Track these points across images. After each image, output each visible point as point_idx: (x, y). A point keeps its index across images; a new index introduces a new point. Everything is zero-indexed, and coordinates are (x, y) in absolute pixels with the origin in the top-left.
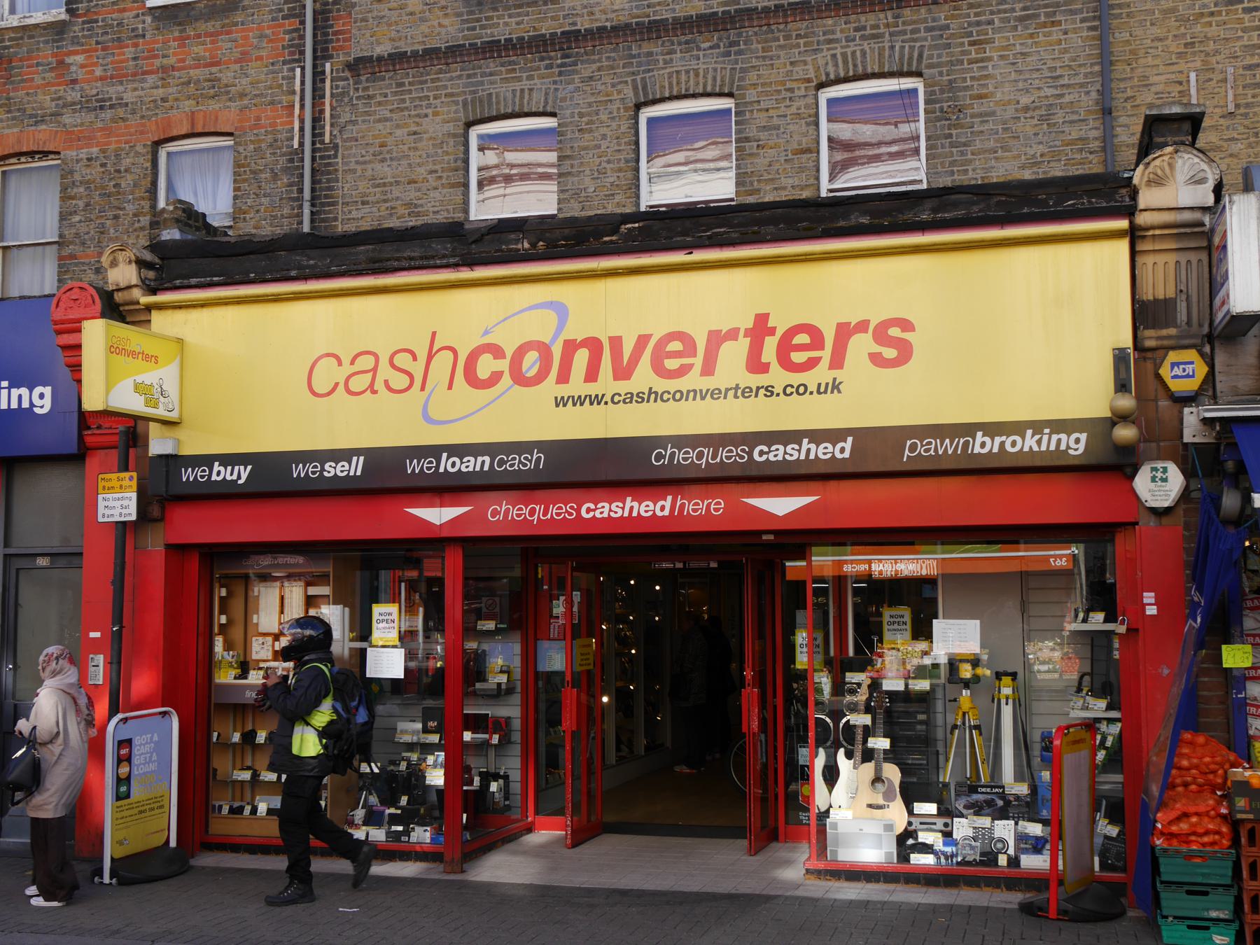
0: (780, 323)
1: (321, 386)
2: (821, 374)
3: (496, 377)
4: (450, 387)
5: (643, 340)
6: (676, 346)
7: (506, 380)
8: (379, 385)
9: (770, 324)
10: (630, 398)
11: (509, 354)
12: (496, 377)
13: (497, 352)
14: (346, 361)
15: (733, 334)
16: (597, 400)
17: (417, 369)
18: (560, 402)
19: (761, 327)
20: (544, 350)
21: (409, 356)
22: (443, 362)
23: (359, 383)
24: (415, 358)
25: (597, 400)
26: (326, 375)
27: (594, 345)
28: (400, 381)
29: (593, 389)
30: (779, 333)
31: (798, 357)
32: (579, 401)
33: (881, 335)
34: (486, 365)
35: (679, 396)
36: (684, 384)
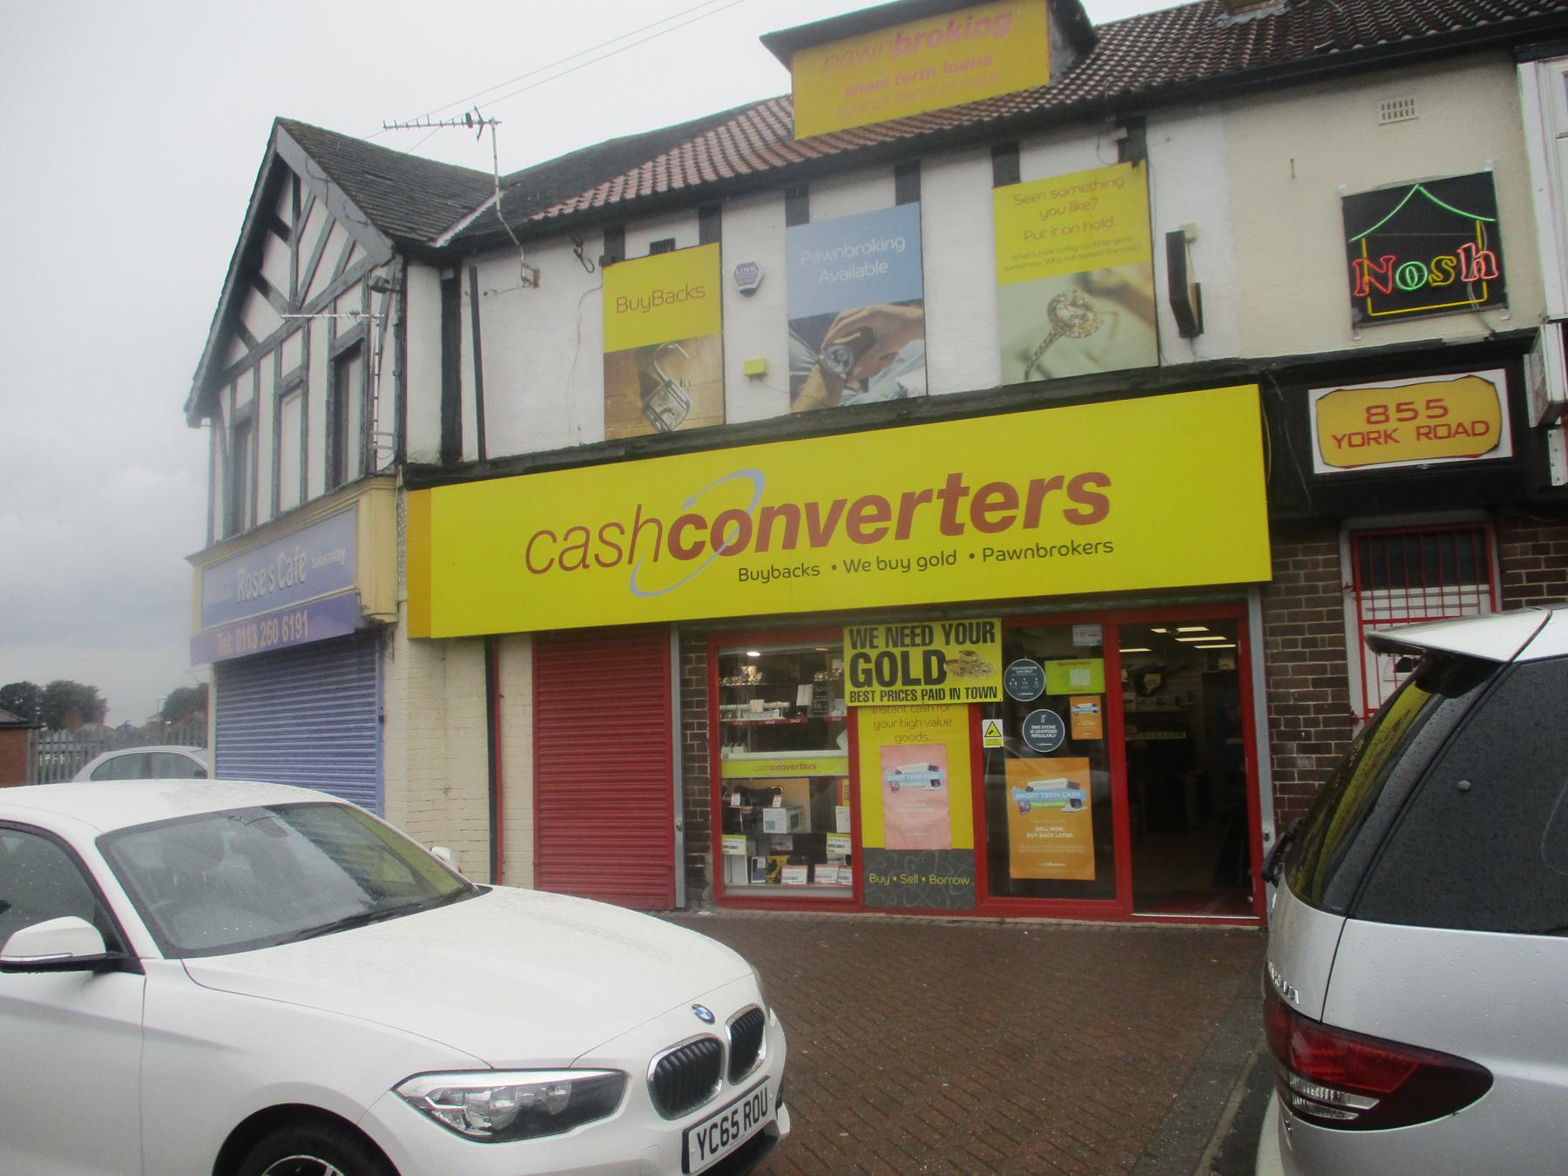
0: (974, 482)
1: (538, 564)
3: (698, 548)
4: (656, 559)
5: (838, 506)
6: (870, 510)
8: (590, 560)
9: (963, 485)
11: (710, 526)
12: (698, 548)
13: (698, 522)
14: (560, 537)
17: (625, 542)
19: (954, 489)
20: (741, 517)
21: (615, 530)
23: (572, 558)
24: (622, 532)
26: (544, 551)
27: (790, 511)
28: (609, 555)
30: (972, 493)
33: (1076, 491)
34: (689, 536)
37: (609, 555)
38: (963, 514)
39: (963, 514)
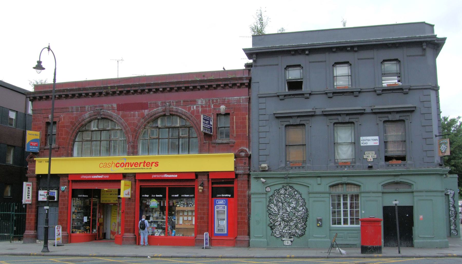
0: (146, 162)
2: (150, 167)
3: (119, 166)
5: (133, 163)
7: (120, 166)
8: (107, 166)
10: (132, 169)
12: (119, 166)
13: (119, 164)
15: (142, 163)
16: (128, 169)
17: (111, 165)
18: (125, 169)
19: (145, 162)
20: (124, 163)
22: (113, 164)
23: (105, 166)
25: (128, 169)
26: (101, 165)
28: (109, 166)
29: (128, 168)
31: (148, 165)
32: (127, 169)
33: (156, 163)
35: (136, 169)
36: (137, 168)
37: (109, 166)
38: (145, 165)
39: (145, 165)
